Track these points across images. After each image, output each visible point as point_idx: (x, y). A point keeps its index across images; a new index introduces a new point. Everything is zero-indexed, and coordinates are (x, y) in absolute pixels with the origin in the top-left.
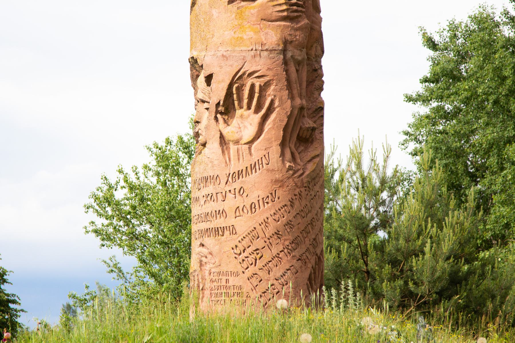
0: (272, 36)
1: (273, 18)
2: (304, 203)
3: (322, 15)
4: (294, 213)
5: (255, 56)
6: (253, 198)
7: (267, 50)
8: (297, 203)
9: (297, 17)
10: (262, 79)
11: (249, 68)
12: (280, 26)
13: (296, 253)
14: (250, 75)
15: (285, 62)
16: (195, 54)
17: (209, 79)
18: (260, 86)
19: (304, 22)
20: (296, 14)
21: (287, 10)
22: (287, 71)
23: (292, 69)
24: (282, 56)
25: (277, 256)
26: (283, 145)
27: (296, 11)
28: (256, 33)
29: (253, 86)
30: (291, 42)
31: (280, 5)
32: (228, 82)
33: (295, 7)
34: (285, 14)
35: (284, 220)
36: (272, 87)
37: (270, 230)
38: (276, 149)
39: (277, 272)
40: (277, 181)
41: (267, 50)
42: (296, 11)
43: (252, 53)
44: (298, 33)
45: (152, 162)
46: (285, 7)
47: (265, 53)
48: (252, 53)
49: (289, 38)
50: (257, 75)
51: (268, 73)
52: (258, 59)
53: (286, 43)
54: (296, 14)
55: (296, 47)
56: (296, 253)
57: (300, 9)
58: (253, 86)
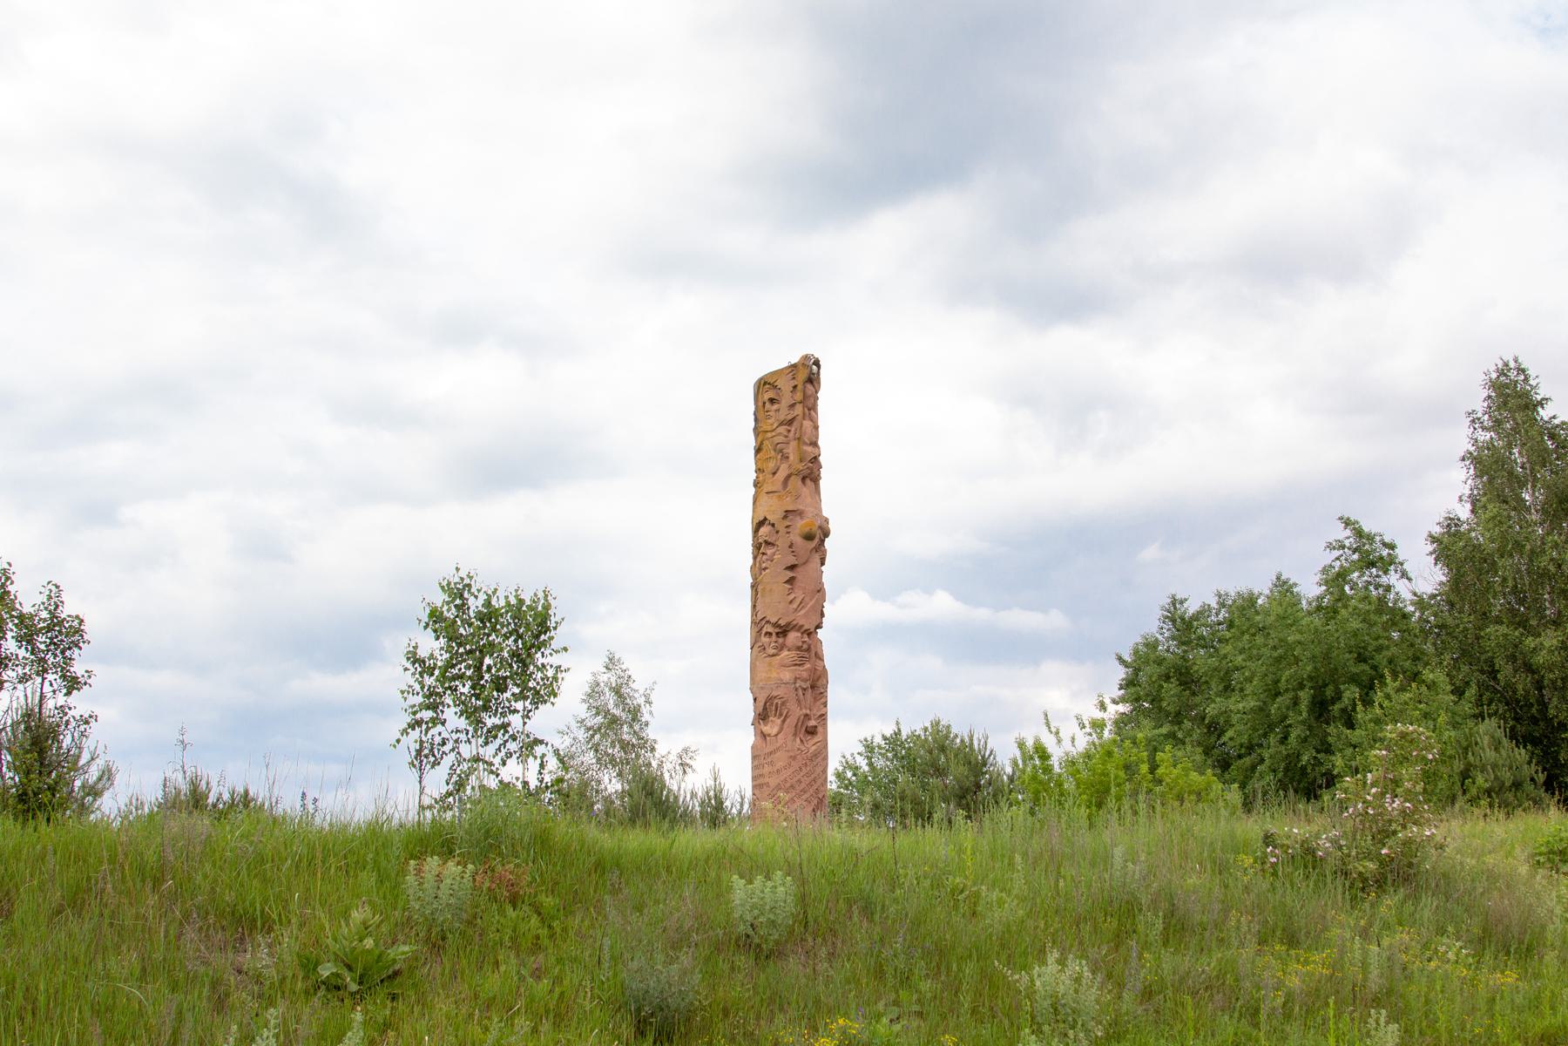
6: (779, 765)
11: (775, 693)
19: (808, 666)
26: (795, 735)
38: (791, 737)
45: (862, 749)
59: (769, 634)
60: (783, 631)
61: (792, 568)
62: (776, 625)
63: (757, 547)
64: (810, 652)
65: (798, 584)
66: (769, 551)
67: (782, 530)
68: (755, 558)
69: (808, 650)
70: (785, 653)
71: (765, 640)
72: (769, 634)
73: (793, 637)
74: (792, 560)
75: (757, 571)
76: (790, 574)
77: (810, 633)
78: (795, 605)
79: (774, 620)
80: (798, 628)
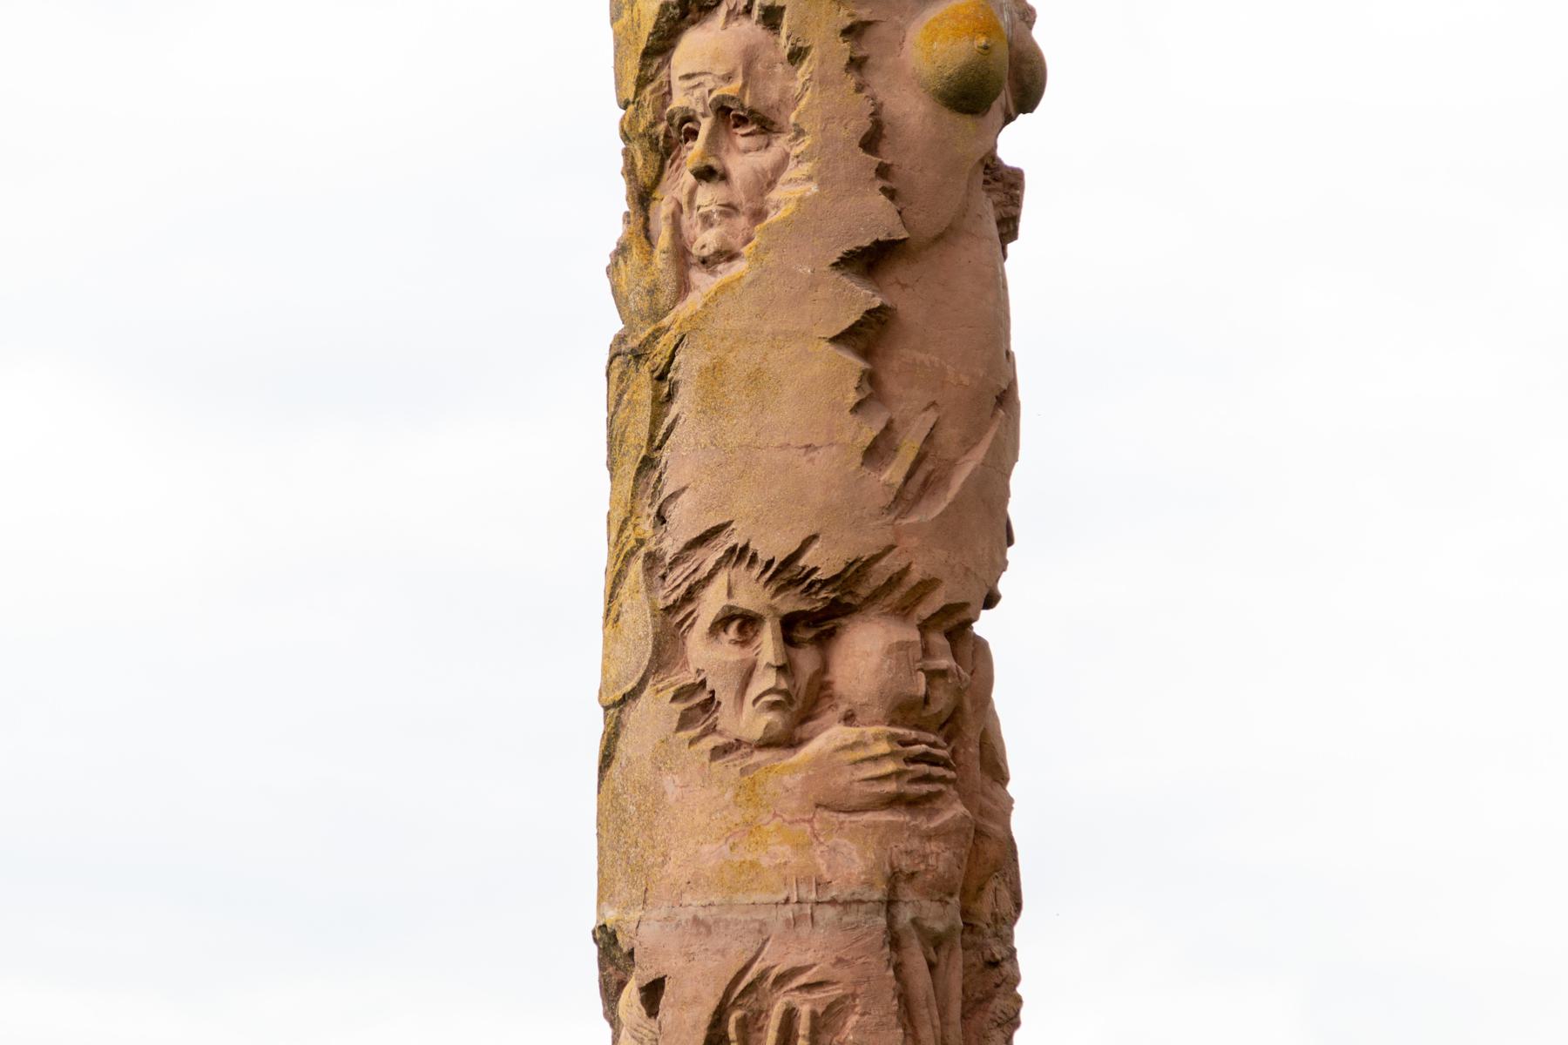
0: (851, 858)
1: (853, 803)
3: (1011, 788)
5: (796, 921)
7: (833, 902)
9: (929, 797)
10: (818, 995)
11: (776, 958)
12: (875, 826)
14: (782, 979)
15: (894, 941)
16: (611, 916)
17: (653, 993)
18: (814, 1016)
19: (953, 811)
20: (925, 788)
21: (898, 775)
22: (898, 968)
23: (916, 960)
24: (882, 921)
27: (927, 779)
28: (798, 847)
29: (790, 1016)
31: (875, 759)
32: (713, 1003)
33: (923, 768)
34: (891, 787)
36: (853, 1020)
41: (833, 902)
42: (927, 779)
43: (788, 912)
44: (932, 847)
46: (889, 767)
47: (830, 913)
48: (788, 912)
49: (905, 864)
50: (803, 979)
51: (838, 973)
52: (804, 930)
53: (895, 879)
54: (925, 788)
55: (926, 892)
57: (938, 771)
58: (790, 1016)
59: (743, 623)
60: (816, 615)
61: (869, 261)
62: (785, 574)
63: (656, 144)
64: (950, 743)
65: (903, 357)
66: (744, 159)
67: (828, 49)
68: (642, 198)
69: (950, 725)
70: (829, 736)
71: (707, 655)
72: (743, 623)
73: (866, 653)
74: (874, 218)
75: (658, 256)
76: (860, 297)
77: (955, 627)
78: (894, 473)
79: (774, 545)
80: (899, 594)
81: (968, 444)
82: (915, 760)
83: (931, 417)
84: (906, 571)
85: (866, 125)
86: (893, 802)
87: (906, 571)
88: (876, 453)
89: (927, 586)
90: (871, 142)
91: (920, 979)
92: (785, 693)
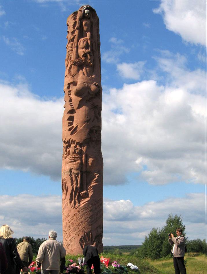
2: (77, 217)
4: (74, 220)
8: (75, 217)
13: (75, 232)
25: (70, 233)
30: (73, 169)
33: (74, 158)
34: (70, 160)
35: (71, 222)
37: (68, 225)
38: (69, 201)
39: (70, 238)
40: (69, 211)
44: (74, 165)
47: (66, 173)
49: (72, 168)
55: (75, 169)
56: (75, 232)
81: (81, 127)
82: (74, 157)
83: (77, 125)
84: (72, 140)
85: (69, 100)
86: (71, 162)
87: (72, 140)
88: (70, 130)
89: (75, 141)
90: (70, 101)
91: (74, 178)
92: (66, 153)
